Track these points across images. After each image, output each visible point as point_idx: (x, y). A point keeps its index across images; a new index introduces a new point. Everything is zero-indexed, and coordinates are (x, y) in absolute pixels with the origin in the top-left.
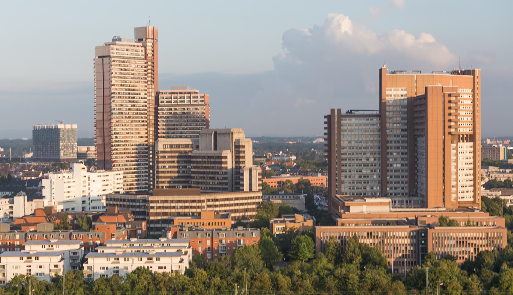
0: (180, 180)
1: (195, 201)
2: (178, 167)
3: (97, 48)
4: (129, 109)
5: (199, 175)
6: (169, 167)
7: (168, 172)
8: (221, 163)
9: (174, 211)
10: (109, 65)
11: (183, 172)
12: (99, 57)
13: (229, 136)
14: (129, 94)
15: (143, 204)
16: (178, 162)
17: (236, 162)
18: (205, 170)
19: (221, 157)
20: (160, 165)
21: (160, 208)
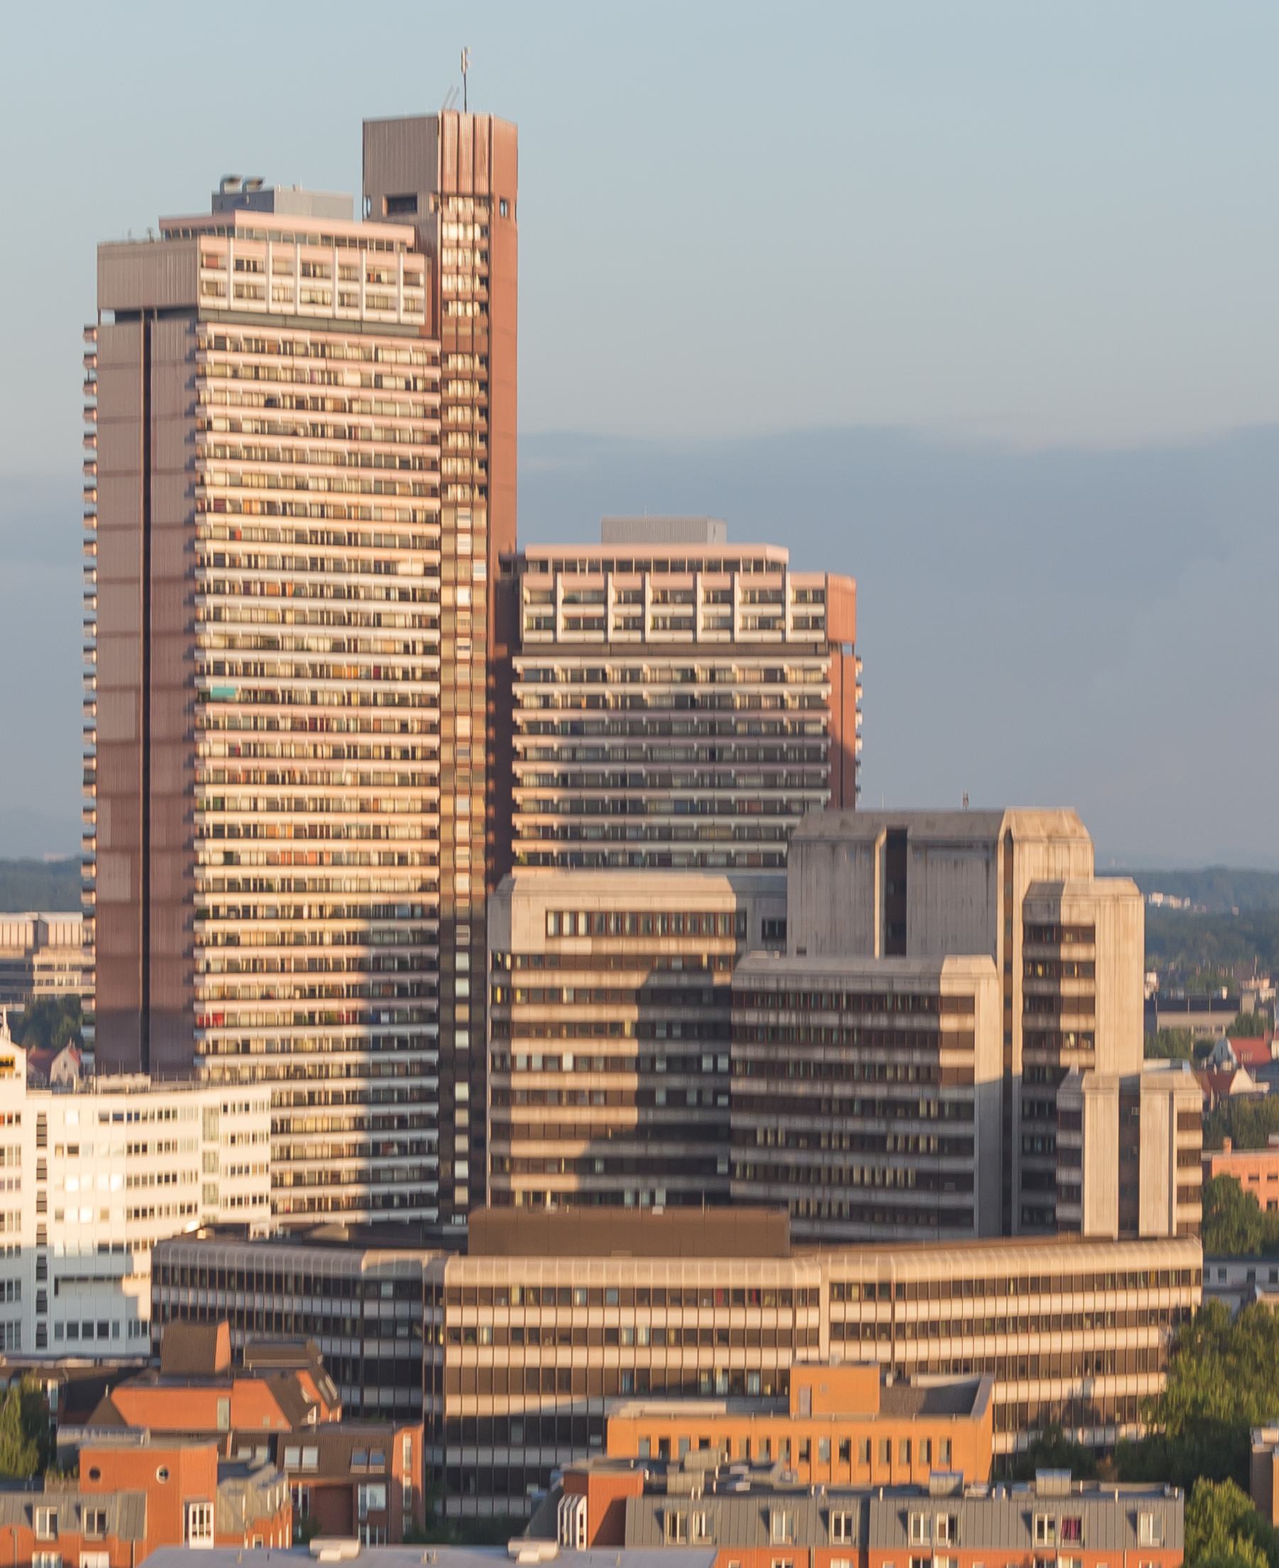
0: (654, 1150)
1: (755, 1297)
2: (641, 1065)
3: (107, 253)
4: (320, 672)
5: (785, 1123)
6: (585, 1064)
7: (574, 1098)
8: (933, 1040)
9: (611, 1357)
10: (186, 371)
12: (123, 316)
13: (990, 864)
14: (316, 565)
15: (403, 1309)
16: (643, 1031)
17: (1033, 1039)
18: (821, 1089)
19: (934, 1004)
20: (520, 1047)
21: (517, 1336)
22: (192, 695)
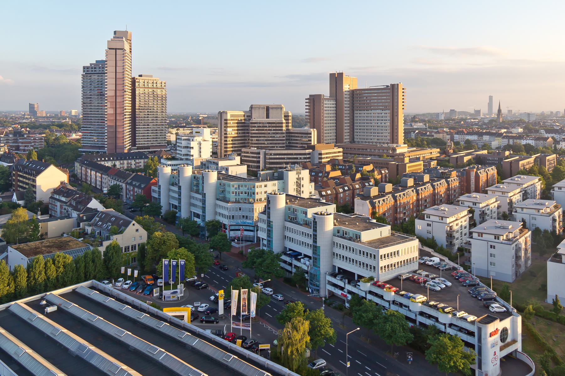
3: (108, 41)
10: (123, 56)
11: (240, 133)
12: (110, 49)
16: (237, 127)
19: (282, 123)
22: (124, 91)
